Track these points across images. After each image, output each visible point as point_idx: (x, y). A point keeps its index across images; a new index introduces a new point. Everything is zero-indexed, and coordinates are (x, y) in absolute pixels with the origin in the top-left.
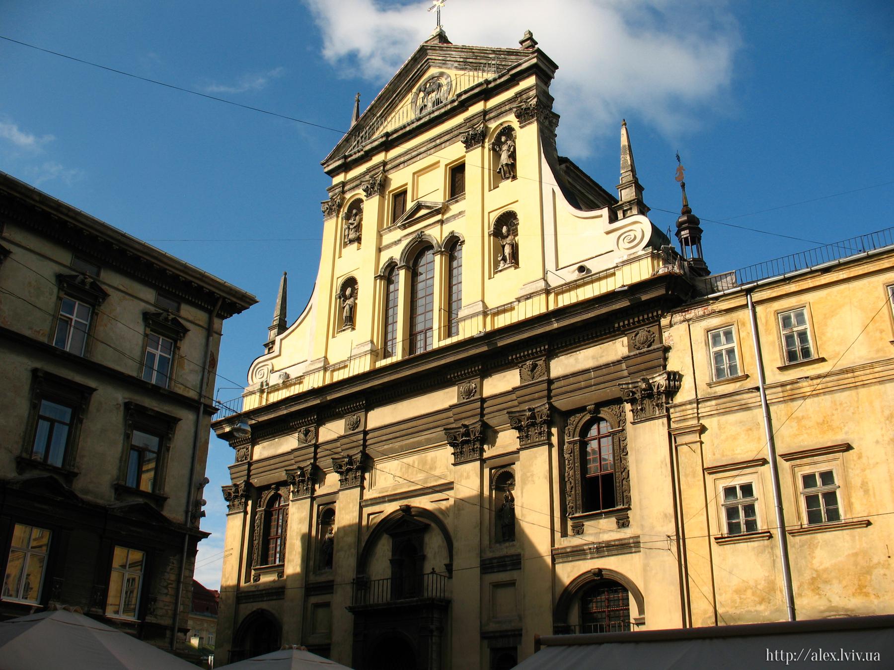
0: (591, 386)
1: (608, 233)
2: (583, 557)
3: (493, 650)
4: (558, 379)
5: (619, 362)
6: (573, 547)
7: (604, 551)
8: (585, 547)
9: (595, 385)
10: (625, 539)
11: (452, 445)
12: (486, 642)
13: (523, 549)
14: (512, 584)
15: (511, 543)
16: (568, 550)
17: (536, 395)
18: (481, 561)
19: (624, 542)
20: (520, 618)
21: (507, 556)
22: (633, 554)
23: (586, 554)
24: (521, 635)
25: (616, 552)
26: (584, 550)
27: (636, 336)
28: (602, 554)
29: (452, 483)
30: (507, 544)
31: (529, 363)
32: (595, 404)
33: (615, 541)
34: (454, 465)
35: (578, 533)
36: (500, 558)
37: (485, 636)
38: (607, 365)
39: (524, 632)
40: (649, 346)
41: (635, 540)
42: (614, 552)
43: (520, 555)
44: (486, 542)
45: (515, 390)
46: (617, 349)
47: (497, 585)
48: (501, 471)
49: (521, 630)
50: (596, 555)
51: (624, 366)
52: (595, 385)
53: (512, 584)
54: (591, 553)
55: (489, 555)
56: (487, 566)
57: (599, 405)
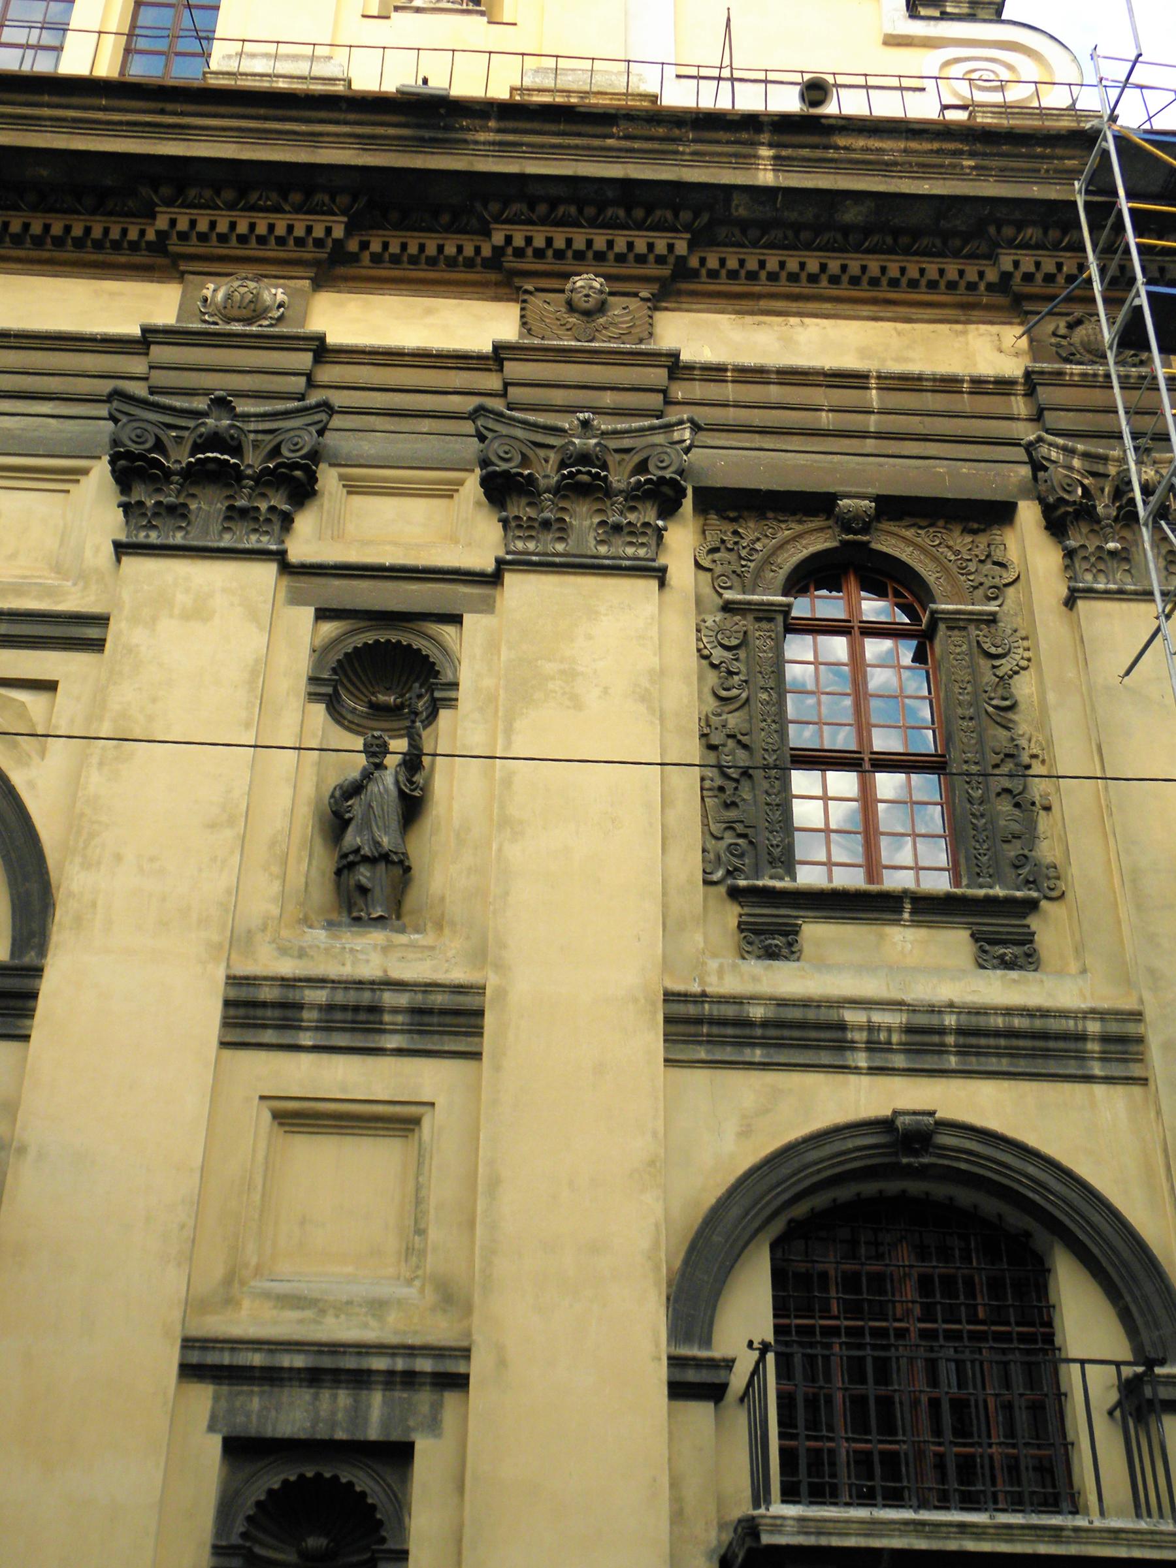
0: (864, 435)
1: (894, 41)
2: (825, 1058)
3: (241, 1449)
4: (714, 372)
5: (1003, 385)
6: (783, 1003)
7: (941, 1050)
8: (852, 1016)
9: (880, 436)
10: (1063, 1014)
11: (131, 470)
12: (203, 1396)
13: (499, 967)
14: (399, 1121)
15: (402, 939)
16: (757, 1012)
17: (608, 399)
18: (234, 981)
19: (1054, 1025)
20: (451, 1297)
21: (399, 986)
22: (1099, 1090)
23: (844, 1046)
24: (460, 1382)
25: (1004, 1064)
26: (842, 1026)
27: (1071, 326)
28: (930, 1062)
29: (102, 620)
30: (377, 936)
31: (588, 283)
32: (879, 499)
33: (1009, 1012)
34: (121, 549)
35: (771, 954)
36: (359, 984)
37: (205, 1363)
38: (948, 384)
39: (478, 1368)
41: (1114, 1028)
42: (993, 1064)
43: (480, 990)
44: (263, 899)
45: (500, 354)
46: (990, 349)
47: (297, 1117)
48: (370, 638)
49: (465, 1353)
50: (899, 1061)
52: (880, 436)
53: (399, 1121)
54: (873, 1047)
55: (270, 962)
56: (257, 1014)
57: (895, 508)
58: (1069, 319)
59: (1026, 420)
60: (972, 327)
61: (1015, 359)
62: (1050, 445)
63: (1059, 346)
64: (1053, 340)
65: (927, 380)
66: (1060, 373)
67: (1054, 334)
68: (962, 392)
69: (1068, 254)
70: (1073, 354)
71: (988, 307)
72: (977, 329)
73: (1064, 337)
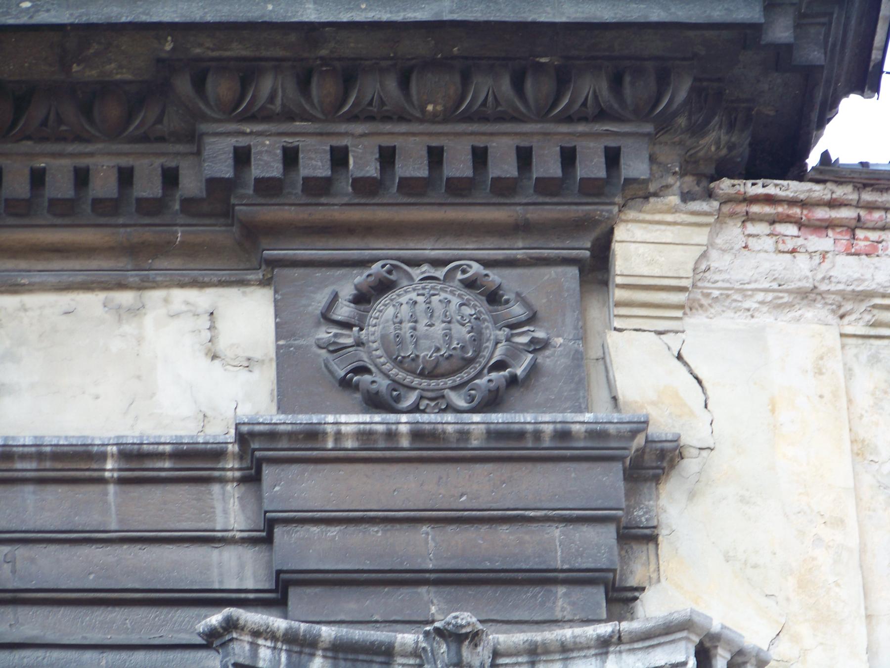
5: (192, 463)
27: (363, 299)
40: (492, 402)
51: (229, 508)
58: (360, 277)
59: (243, 541)
60: (155, 296)
61: (243, 375)
62: (256, 634)
63: (336, 349)
64: (325, 333)
65: (24, 457)
66: (313, 435)
67: (326, 318)
68: (102, 481)
69: (359, 128)
70: (362, 370)
71: (190, 251)
72: (166, 301)
73: (346, 325)
